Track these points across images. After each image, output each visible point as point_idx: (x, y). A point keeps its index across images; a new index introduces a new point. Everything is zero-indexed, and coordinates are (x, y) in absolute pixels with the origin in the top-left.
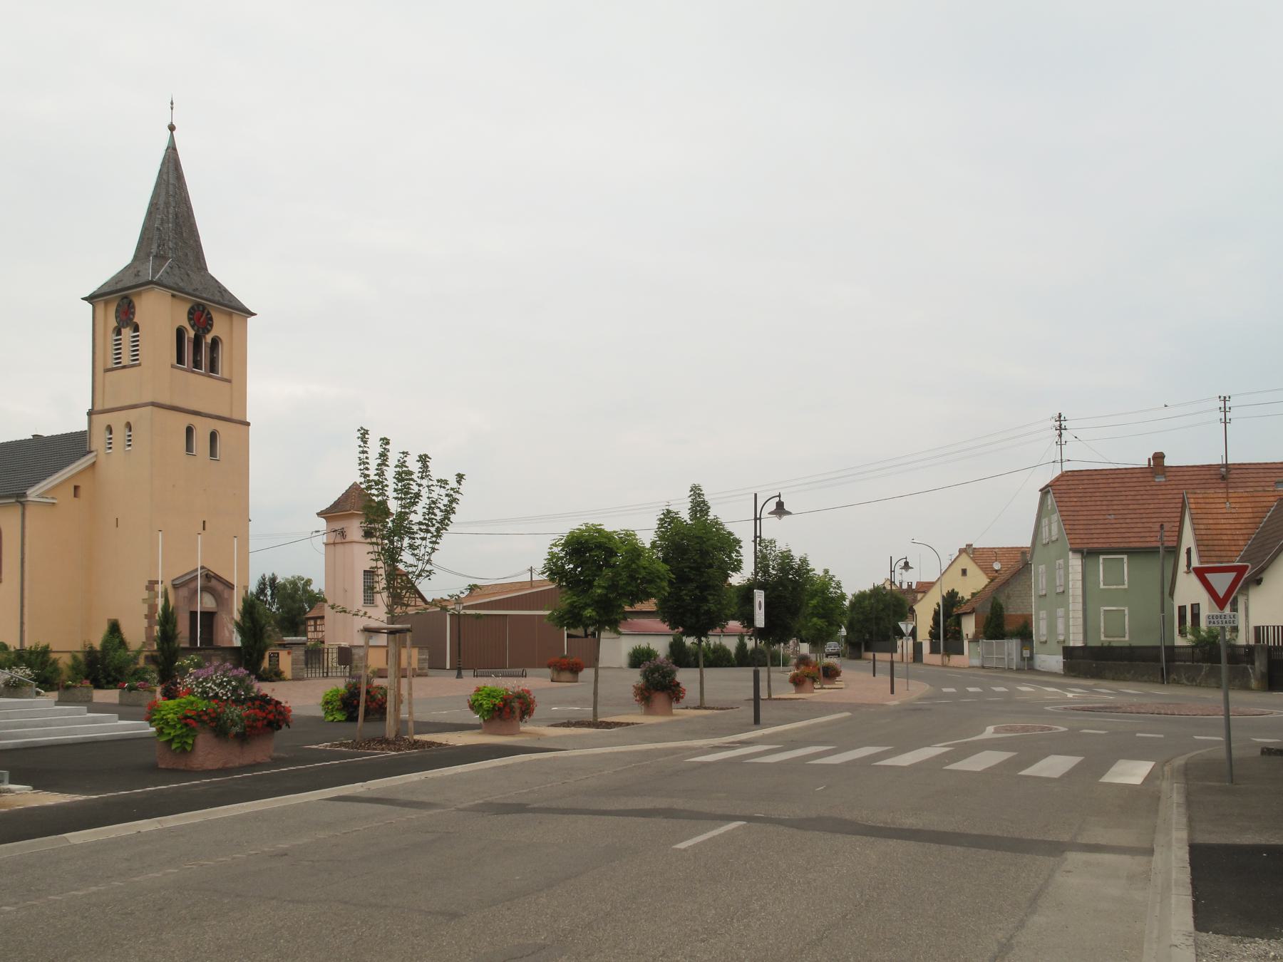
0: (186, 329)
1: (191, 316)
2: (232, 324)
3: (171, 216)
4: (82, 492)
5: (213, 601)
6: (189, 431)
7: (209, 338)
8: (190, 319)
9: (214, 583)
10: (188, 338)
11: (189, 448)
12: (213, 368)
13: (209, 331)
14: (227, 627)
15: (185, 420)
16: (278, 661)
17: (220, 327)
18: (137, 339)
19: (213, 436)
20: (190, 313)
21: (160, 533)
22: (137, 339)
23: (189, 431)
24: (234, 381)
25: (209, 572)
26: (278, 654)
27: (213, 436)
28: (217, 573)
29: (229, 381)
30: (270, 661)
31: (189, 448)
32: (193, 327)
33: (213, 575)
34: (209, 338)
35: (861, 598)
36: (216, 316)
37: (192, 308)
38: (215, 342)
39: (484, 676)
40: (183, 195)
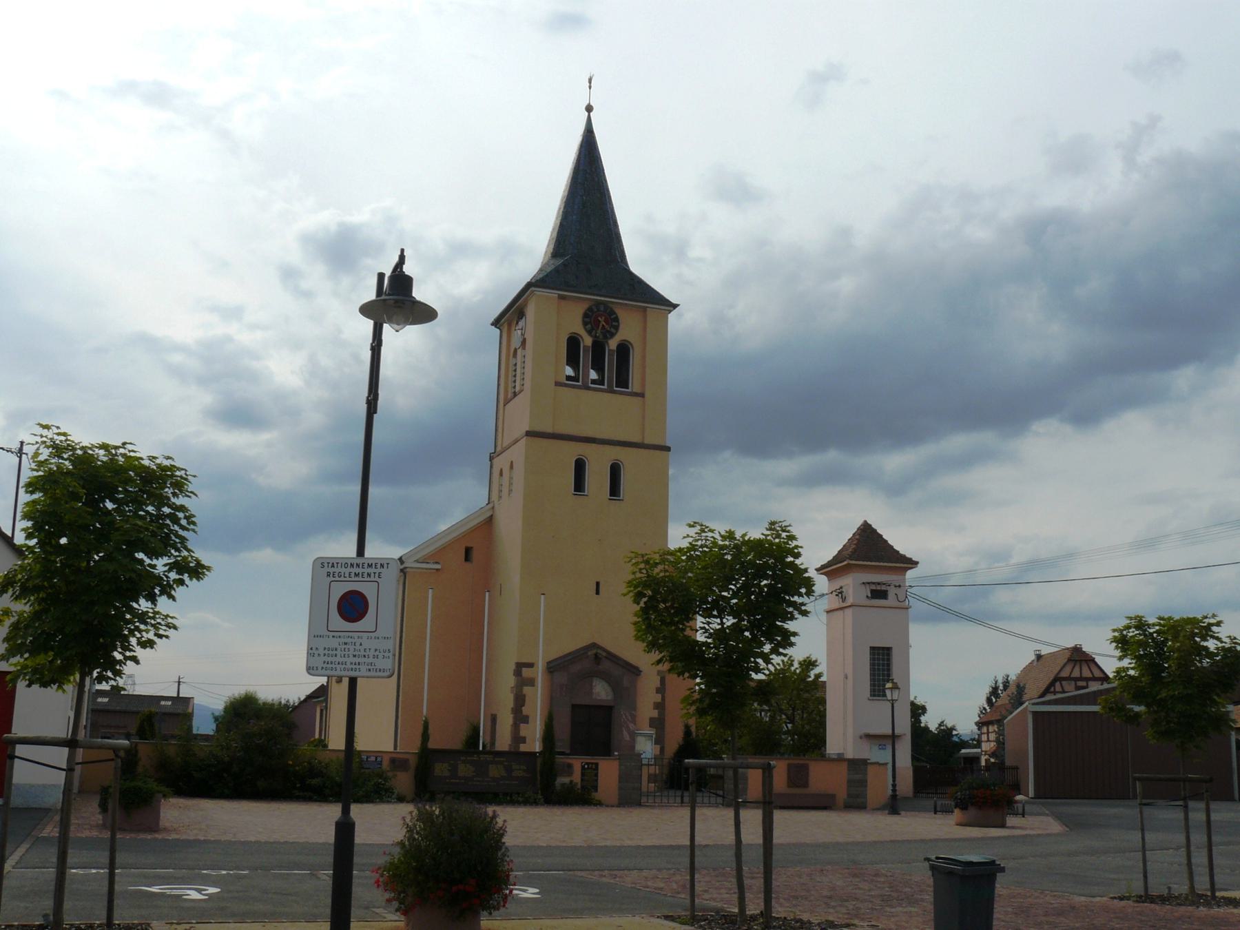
0: (580, 336)
1: (587, 320)
2: (645, 322)
3: (576, 207)
4: (475, 555)
5: (609, 689)
6: (580, 466)
7: (613, 344)
8: (585, 324)
9: (606, 665)
10: (584, 346)
11: (579, 486)
12: (623, 381)
13: (612, 335)
14: (628, 727)
15: (572, 451)
16: (596, 775)
17: (628, 330)
18: (378, 325)
19: (615, 471)
20: (586, 315)
21: (542, 596)
22: (378, 325)
23: (580, 466)
24: (647, 394)
25: (599, 651)
26: (597, 764)
27: (615, 471)
28: (612, 651)
29: (642, 395)
30: (583, 774)
31: (579, 486)
32: (589, 332)
33: (604, 654)
34: (613, 344)
35: (996, 875)
36: (622, 314)
37: (590, 309)
38: (624, 351)
39: (903, 841)
40: (596, 179)
